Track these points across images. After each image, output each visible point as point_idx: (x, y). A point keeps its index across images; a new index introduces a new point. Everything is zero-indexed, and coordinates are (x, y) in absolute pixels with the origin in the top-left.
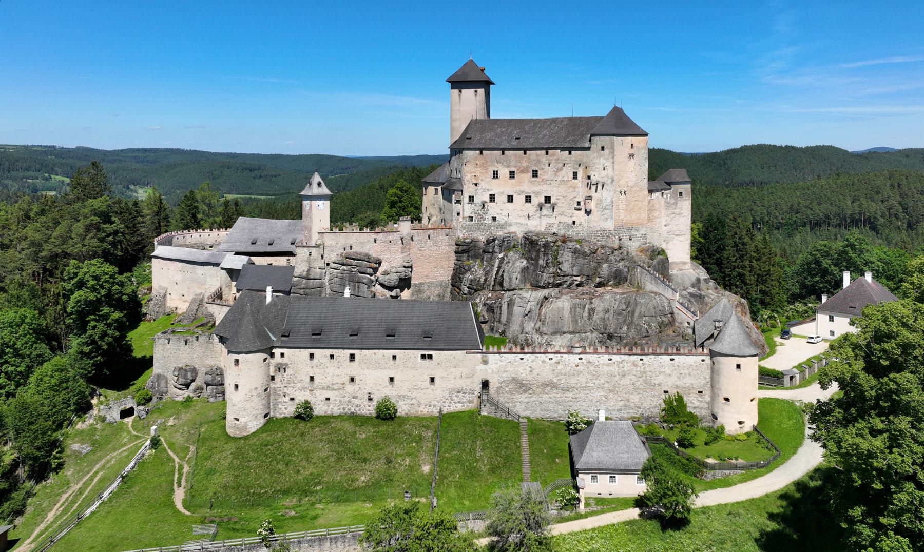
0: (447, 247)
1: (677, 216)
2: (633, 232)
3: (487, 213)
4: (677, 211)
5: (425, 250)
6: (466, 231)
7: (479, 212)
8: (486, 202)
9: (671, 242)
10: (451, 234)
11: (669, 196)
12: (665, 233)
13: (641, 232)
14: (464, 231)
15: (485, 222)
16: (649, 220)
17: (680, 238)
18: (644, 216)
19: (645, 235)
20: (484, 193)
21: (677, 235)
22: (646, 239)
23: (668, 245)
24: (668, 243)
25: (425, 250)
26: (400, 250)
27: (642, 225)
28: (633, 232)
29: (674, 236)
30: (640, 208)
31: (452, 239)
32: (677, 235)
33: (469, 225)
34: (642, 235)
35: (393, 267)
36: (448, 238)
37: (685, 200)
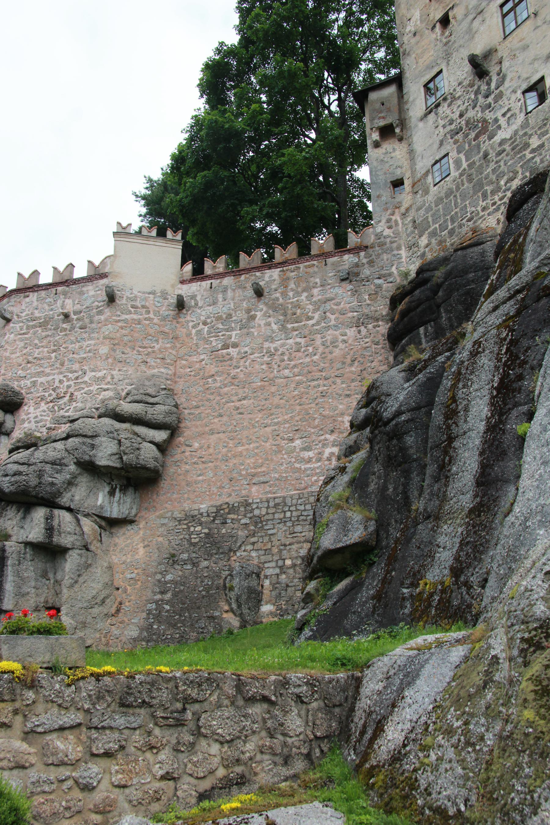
0: (351, 332)
3: (500, 96)
5: (244, 356)
6: (434, 234)
7: (471, 114)
8: (489, 54)
10: (366, 272)
14: (424, 241)
15: (501, 135)
20: (476, 23)
25: (244, 356)
26: (104, 350)
31: (373, 296)
33: (439, 201)
35: (58, 421)
36: (355, 292)
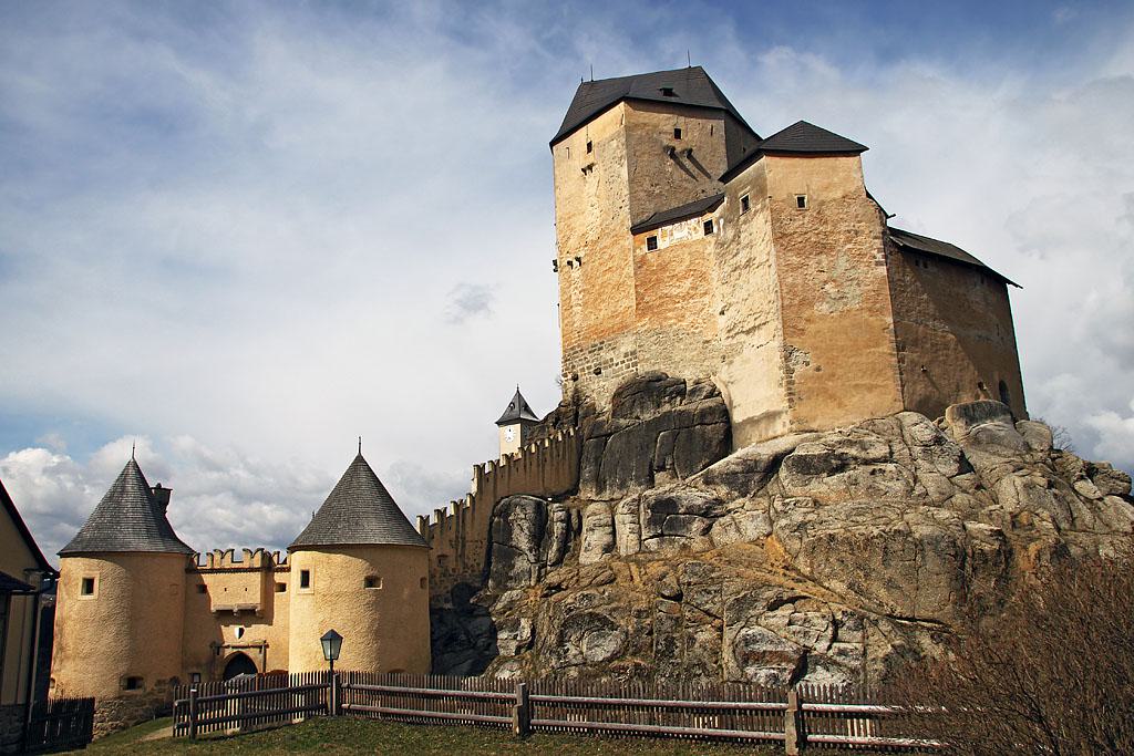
1: (744, 272)
2: (606, 355)
4: (742, 258)
9: (737, 359)
11: (722, 221)
12: (724, 336)
13: (623, 350)
16: (643, 309)
17: (757, 338)
18: (626, 303)
19: (633, 353)
21: (748, 332)
22: (635, 364)
23: (732, 368)
24: (731, 362)
27: (623, 329)
28: (606, 355)
29: (742, 337)
30: (619, 286)
32: (748, 332)
34: (626, 355)
37: (756, 212)
